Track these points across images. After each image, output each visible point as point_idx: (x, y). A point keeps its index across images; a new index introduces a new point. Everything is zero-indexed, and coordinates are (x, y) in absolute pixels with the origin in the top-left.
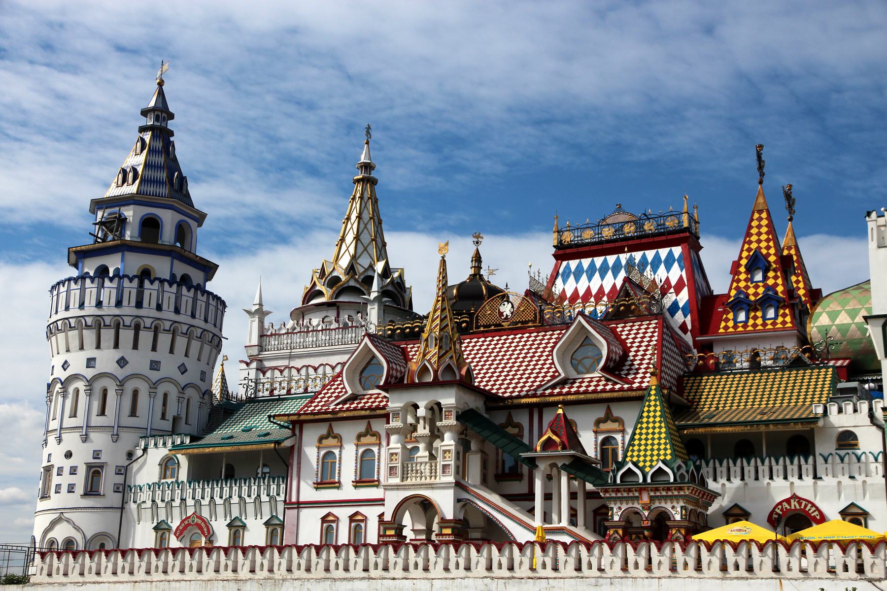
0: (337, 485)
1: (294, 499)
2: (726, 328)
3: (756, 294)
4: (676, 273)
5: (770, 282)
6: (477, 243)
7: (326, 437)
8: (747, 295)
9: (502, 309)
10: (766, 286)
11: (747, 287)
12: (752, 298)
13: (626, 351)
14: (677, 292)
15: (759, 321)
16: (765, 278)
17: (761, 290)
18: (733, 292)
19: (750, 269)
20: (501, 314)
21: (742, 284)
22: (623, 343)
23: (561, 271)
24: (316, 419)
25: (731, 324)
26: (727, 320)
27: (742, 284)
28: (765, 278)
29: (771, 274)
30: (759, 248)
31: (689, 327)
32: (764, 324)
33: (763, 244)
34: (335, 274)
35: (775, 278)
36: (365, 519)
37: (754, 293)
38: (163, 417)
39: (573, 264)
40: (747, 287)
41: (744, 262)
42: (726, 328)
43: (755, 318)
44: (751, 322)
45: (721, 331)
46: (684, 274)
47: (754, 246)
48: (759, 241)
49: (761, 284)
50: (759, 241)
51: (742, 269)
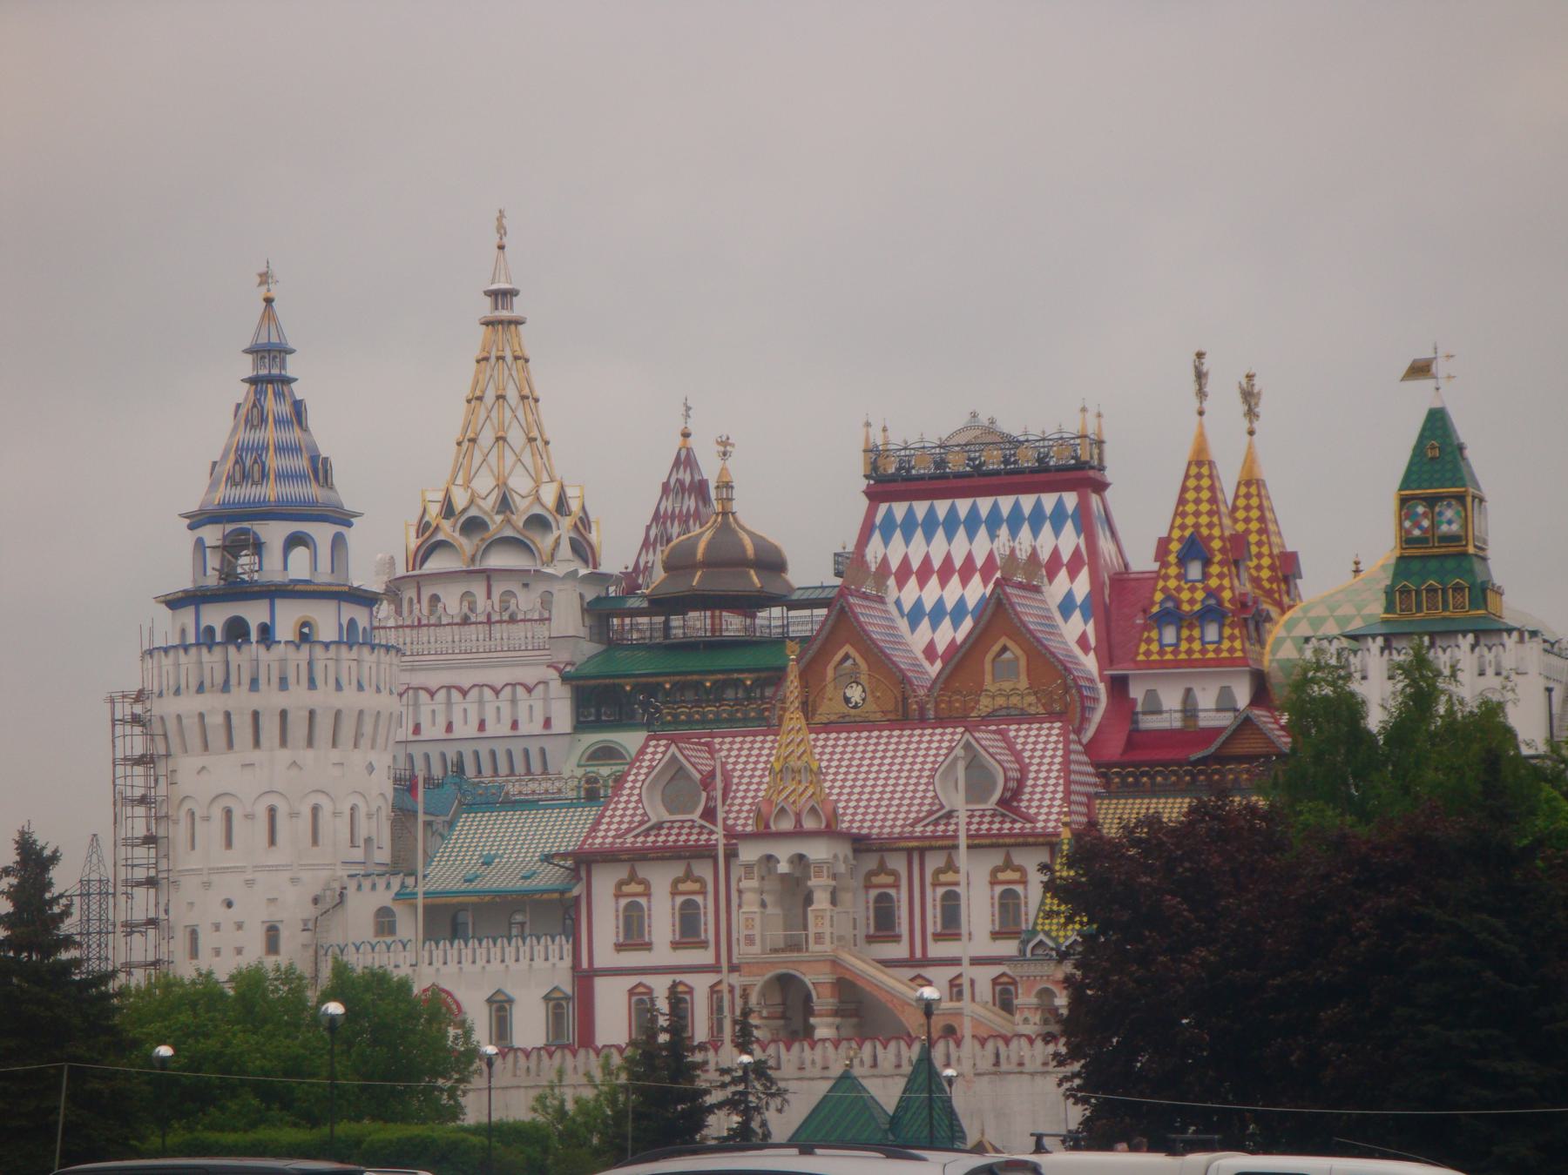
0: (648, 946)
1: (585, 965)
2: (1148, 653)
3: (1192, 602)
4: (1069, 541)
5: (1213, 583)
6: (725, 454)
7: (627, 883)
8: (1178, 603)
9: (849, 693)
10: (1207, 589)
11: (1179, 589)
12: (1186, 607)
13: (1024, 770)
14: (1073, 575)
15: (1197, 646)
16: (1206, 576)
17: (1200, 595)
18: (1159, 596)
19: (1182, 561)
20: (847, 700)
21: (1172, 584)
22: (1018, 756)
23: (878, 519)
24: (609, 857)
25: (1155, 647)
26: (1149, 641)
27: (1172, 584)
28: (1206, 576)
29: (1215, 569)
30: (1197, 526)
31: (1092, 641)
32: (1203, 651)
33: (1204, 520)
34: (473, 512)
35: (1221, 576)
36: (691, 991)
37: (1192, 599)
38: (353, 845)
39: (900, 509)
40: (1179, 589)
41: (1175, 546)
42: (1148, 653)
43: (1190, 639)
44: (1184, 646)
45: (1141, 658)
46: (1082, 541)
47: (1190, 521)
48: (1197, 514)
49: (1199, 585)
50: (1197, 514)
51: (1172, 559)
